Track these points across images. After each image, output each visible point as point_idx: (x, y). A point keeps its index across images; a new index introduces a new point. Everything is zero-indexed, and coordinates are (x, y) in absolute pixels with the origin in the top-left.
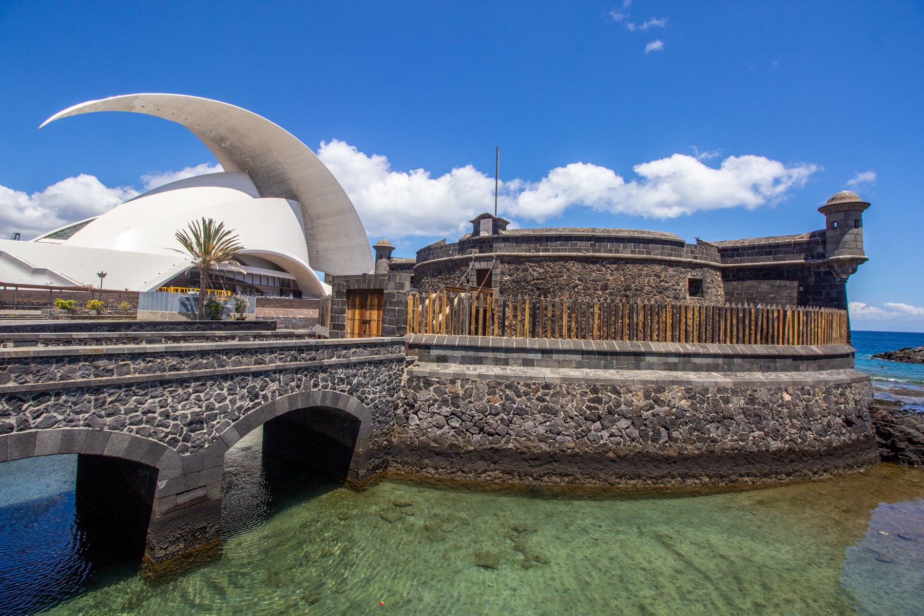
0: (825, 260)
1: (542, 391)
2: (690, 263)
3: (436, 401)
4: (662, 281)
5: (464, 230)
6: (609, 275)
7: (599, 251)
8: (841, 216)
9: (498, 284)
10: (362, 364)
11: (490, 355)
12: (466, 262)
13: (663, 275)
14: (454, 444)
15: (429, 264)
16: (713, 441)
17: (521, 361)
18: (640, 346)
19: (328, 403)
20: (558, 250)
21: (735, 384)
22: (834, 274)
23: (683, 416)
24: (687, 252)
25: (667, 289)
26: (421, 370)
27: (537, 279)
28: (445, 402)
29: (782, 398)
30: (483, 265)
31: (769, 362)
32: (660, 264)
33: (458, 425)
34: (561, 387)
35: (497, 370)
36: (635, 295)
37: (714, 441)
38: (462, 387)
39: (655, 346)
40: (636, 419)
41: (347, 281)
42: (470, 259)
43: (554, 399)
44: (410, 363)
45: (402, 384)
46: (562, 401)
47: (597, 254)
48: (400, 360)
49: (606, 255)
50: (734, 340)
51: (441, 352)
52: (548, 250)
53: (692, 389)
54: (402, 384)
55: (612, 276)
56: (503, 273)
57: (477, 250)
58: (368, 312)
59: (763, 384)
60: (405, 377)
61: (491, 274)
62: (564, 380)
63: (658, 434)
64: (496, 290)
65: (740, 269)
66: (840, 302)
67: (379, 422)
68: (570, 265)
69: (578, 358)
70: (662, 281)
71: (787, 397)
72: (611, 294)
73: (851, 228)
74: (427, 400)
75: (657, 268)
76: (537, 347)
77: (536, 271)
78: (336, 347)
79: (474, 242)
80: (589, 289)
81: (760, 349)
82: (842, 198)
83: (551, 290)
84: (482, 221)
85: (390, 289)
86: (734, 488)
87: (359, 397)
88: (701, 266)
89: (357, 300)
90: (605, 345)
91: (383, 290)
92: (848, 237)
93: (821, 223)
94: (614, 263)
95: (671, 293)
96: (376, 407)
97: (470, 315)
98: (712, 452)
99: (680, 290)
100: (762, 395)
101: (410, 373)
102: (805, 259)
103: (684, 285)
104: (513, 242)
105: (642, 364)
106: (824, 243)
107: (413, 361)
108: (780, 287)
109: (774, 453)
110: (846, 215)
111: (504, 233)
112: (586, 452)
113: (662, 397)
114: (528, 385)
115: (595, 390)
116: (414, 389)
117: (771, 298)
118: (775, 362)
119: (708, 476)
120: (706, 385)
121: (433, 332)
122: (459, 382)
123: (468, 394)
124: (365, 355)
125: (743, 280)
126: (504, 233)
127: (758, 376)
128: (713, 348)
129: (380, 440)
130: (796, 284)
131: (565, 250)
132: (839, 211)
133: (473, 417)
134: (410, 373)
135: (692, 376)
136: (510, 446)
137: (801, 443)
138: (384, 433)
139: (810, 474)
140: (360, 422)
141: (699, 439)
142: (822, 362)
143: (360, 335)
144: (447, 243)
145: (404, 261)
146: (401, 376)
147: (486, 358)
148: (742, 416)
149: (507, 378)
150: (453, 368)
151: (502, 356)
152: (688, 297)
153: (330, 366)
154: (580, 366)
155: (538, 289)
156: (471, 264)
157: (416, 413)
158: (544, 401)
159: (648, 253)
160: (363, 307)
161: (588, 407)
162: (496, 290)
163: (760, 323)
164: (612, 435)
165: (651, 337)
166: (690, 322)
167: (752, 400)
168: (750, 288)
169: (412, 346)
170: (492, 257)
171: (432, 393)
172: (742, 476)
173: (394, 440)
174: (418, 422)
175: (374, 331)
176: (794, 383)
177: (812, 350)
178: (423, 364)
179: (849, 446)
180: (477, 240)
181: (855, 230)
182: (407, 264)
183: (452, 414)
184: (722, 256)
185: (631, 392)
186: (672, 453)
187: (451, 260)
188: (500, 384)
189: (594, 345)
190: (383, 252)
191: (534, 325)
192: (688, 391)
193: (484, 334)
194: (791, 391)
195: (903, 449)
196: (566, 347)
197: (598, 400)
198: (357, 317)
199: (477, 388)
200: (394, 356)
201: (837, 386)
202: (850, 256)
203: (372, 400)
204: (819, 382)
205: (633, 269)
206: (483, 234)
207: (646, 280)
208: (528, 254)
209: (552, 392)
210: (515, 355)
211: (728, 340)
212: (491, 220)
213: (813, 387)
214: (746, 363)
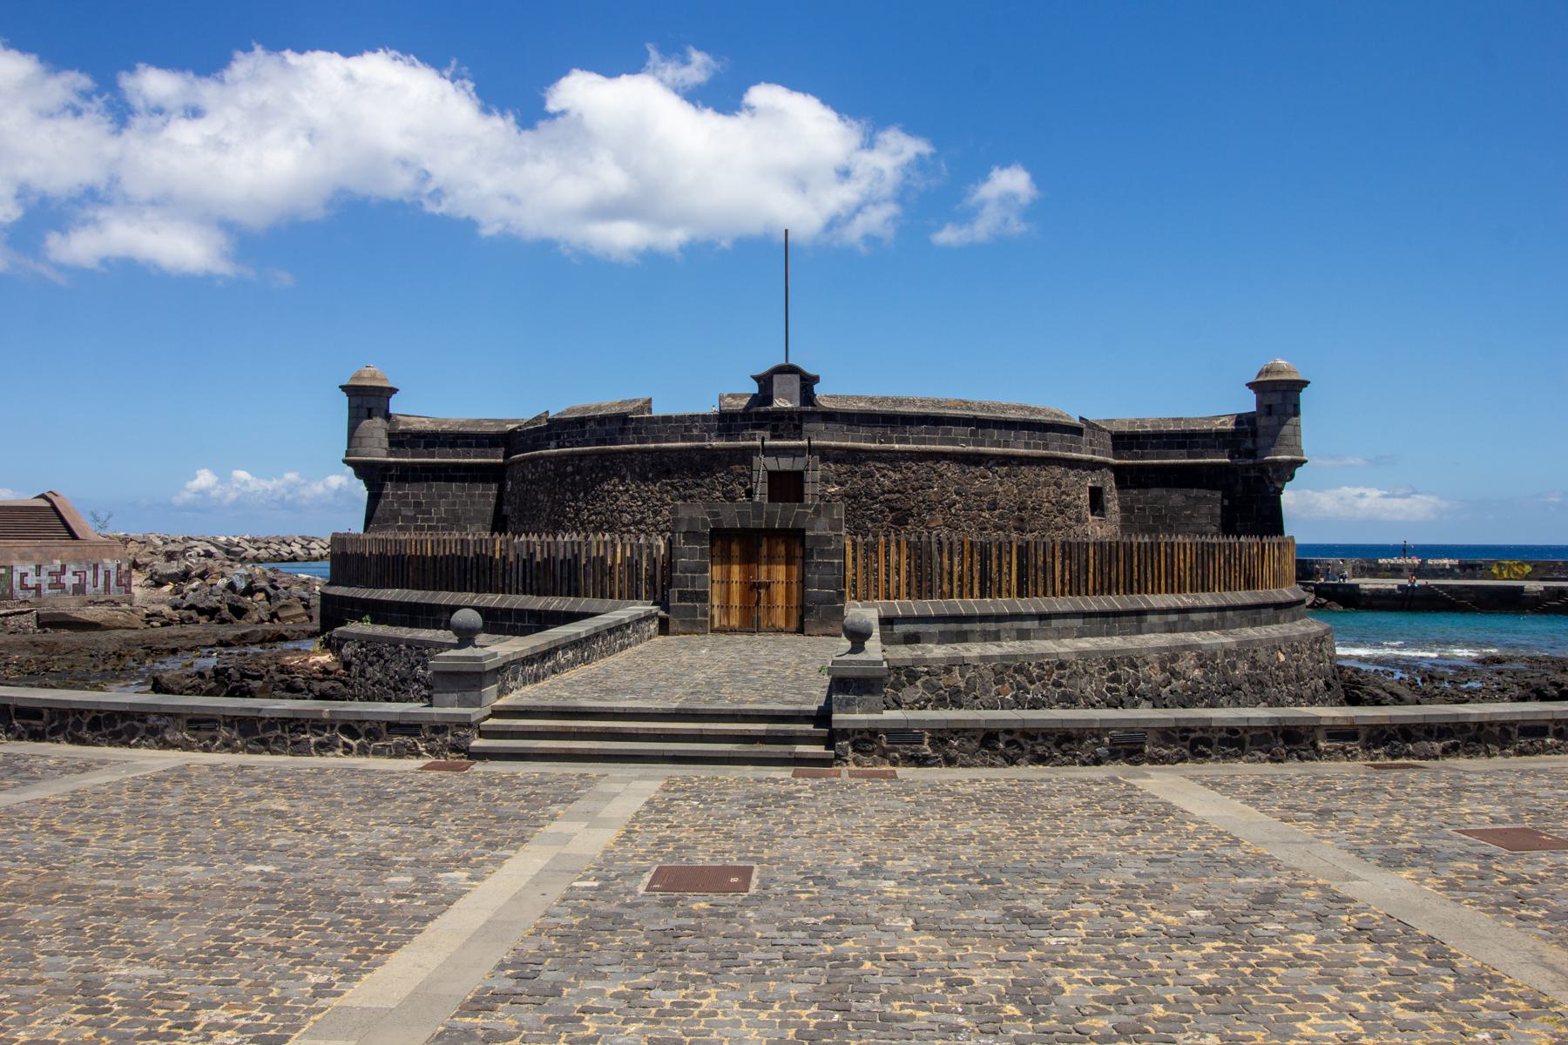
2: (1090, 461)
3: (929, 700)
8: (1275, 399)
11: (977, 627)
15: (630, 452)
21: (1239, 644)
27: (890, 492)
30: (785, 464)
35: (992, 649)
36: (1033, 518)
42: (754, 450)
46: (1082, 683)
47: (982, 449)
49: (994, 450)
52: (906, 441)
55: (1001, 486)
56: (826, 480)
57: (767, 434)
58: (764, 568)
66: (1271, 522)
68: (943, 466)
69: (1078, 622)
75: (1058, 471)
76: (1033, 610)
77: (887, 478)
79: (757, 413)
81: (1244, 597)
82: (1279, 372)
83: (915, 511)
84: (776, 378)
89: (735, 549)
91: (803, 531)
92: (1286, 430)
93: (1248, 403)
94: (1004, 464)
105: (1144, 625)
110: (1279, 397)
114: (1040, 666)
127: (1251, 633)
128: (1206, 599)
130: (1218, 494)
131: (933, 442)
132: (1275, 391)
151: (992, 627)
154: (1081, 634)
155: (892, 510)
158: (1060, 685)
159: (1046, 447)
160: (750, 559)
161: (1109, 689)
176: (1286, 639)
180: (768, 413)
184: (1116, 447)
187: (702, 449)
188: (1007, 667)
192: (1199, 657)
206: (779, 403)
208: (873, 446)
209: (1067, 672)
210: (1007, 625)
212: (795, 381)
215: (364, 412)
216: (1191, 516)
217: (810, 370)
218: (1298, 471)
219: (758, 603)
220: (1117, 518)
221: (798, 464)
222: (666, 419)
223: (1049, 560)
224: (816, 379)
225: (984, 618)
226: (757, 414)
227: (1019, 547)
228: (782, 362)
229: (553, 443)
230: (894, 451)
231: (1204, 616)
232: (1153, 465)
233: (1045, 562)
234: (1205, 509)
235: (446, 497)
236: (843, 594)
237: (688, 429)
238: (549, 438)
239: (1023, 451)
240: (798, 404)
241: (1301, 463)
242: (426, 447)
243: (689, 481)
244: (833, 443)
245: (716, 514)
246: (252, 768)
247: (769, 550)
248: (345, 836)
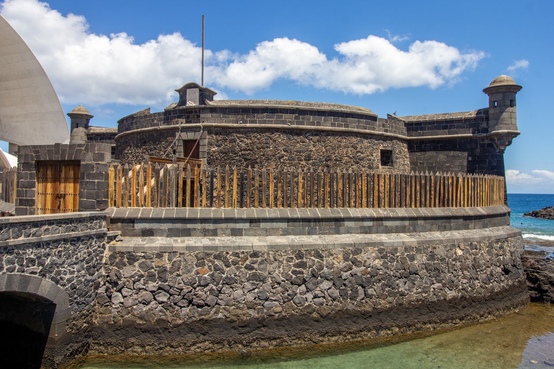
0: (488, 134)
1: (250, 259)
2: (381, 135)
3: (142, 276)
4: (358, 152)
5: (171, 99)
6: (311, 146)
7: (302, 123)
8: (500, 97)
9: (206, 155)
10: (57, 242)
11: (199, 226)
12: (172, 132)
13: (359, 146)
14: (163, 320)
15: (133, 133)
16: (401, 295)
17: (229, 231)
18: (340, 212)
19: (15, 288)
20: (265, 122)
21: (419, 243)
22: (495, 146)
23: (377, 274)
24: (379, 126)
25: (362, 159)
26: (124, 244)
27: (244, 150)
28: (151, 277)
29: (455, 253)
30: (190, 136)
31: (445, 222)
32: (357, 136)
33: (165, 299)
34: (268, 254)
35: (205, 241)
36: (335, 165)
37: (403, 294)
38: (170, 260)
39: (354, 212)
40: (336, 280)
41: (37, 152)
42: (177, 129)
43: (262, 266)
44: (111, 238)
45: (104, 261)
46: (270, 268)
48: (101, 236)
50: (418, 204)
51: (147, 226)
52: (255, 122)
53: (384, 249)
54: (104, 261)
55: (315, 147)
56: (210, 144)
57: (184, 120)
58: (62, 185)
59: (441, 242)
60: (107, 253)
61: (198, 145)
62: (271, 247)
63: (357, 292)
64: (203, 161)
65: (422, 141)
66: (499, 170)
67: (78, 303)
68: (276, 136)
69: (284, 225)
70: (358, 152)
71: (460, 252)
72: (314, 164)
73: (507, 107)
74: (132, 277)
75: (354, 140)
76: (245, 216)
77: (243, 142)
78: (24, 224)
79: (180, 112)
80: (294, 160)
81: (438, 211)
82: (501, 81)
83: (258, 160)
84: (188, 90)
85: (88, 160)
86: (420, 335)
87: (53, 279)
88: (391, 138)
89: (49, 173)
90: (309, 213)
91: (80, 161)
92: (505, 115)
93: (484, 102)
94: (316, 135)
95: (365, 163)
96: (73, 287)
97: (178, 186)
98: (401, 304)
100: (441, 251)
101: (112, 249)
102: (473, 133)
103: (377, 156)
104: (220, 112)
105: (342, 229)
106: (487, 119)
107: (115, 237)
108: (454, 157)
109: (450, 301)
110: (504, 96)
111: (211, 103)
112: (292, 315)
113: (359, 258)
114: (236, 255)
115: (300, 256)
116: (117, 265)
117: (447, 167)
118: (450, 223)
119: (398, 326)
120: (395, 245)
121: (138, 205)
122: (166, 256)
123: (176, 267)
124: (60, 232)
125: (425, 151)
126: (211, 103)
127: (437, 235)
128: (401, 212)
129: (79, 323)
130: (466, 154)
131: (271, 122)
132: (498, 93)
133: (181, 290)
134: (112, 249)
135: (384, 238)
136: (220, 315)
137: (471, 291)
138: (83, 315)
139: (478, 317)
140: (55, 305)
141: (390, 294)
142: (486, 220)
143: (53, 211)
144: (152, 112)
145: (103, 130)
146: (103, 252)
147: (194, 229)
148: (425, 271)
149: (216, 248)
150: (160, 241)
151: (211, 226)
152: (380, 167)
153: (17, 246)
154: (286, 233)
155: (246, 160)
156: (178, 134)
157: (120, 291)
158: (252, 268)
159: (346, 126)
160: (56, 179)
161: (294, 272)
162: (203, 161)
163: (438, 188)
164: (315, 297)
165: (349, 204)
166: (382, 189)
167: (432, 257)
168: (430, 158)
169: (114, 221)
170: (200, 127)
171: (137, 268)
172: (425, 323)
173: (95, 321)
174: (122, 300)
175: (70, 206)
176: (465, 240)
177: (478, 211)
178: (127, 238)
179: (506, 291)
180: (184, 109)
181: (510, 109)
182: (107, 134)
183: (160, 288)
184: (408, 130)
185: (332, 255)
186: (368, 308)
188: (208, 255)
189: (298, 213)
190: (79, 120)
191: (242, 195)
192: (381, 251)
193: (192, 205)
194: (462, 247)
195: (547, 291)
196: (273, 215)
197: (303, 265)
198: (49, 190)
199: (185, 260)
200: (93, 232)
201: (497, 241)
202: (506, 131)
203: (69, 281)
204: (484, 238)
205: (332, 140)
206: (190, 104)
207: (345, 151)
208: (235, 125)
209: (259, 259)
210: (224, 225)
211: (413, 204)
212: (197, 90)
213: (479, 242)
214: (428, 224)
215: (75, 125)
216: (450, 166)
219: (59, 207)
221: (196, 136)
225: (204, 220)
226: (179, 110)
230: (246, 128)
231: (398, 223)
232: (428, 139)
234: (457, 163)
237: (153, 121)
239: (329, 128)
240: (198, 104)
241: (517, 134)
242: (100, 140)
243: (152, 147)
244: (214, 124)
247: (66, 173)
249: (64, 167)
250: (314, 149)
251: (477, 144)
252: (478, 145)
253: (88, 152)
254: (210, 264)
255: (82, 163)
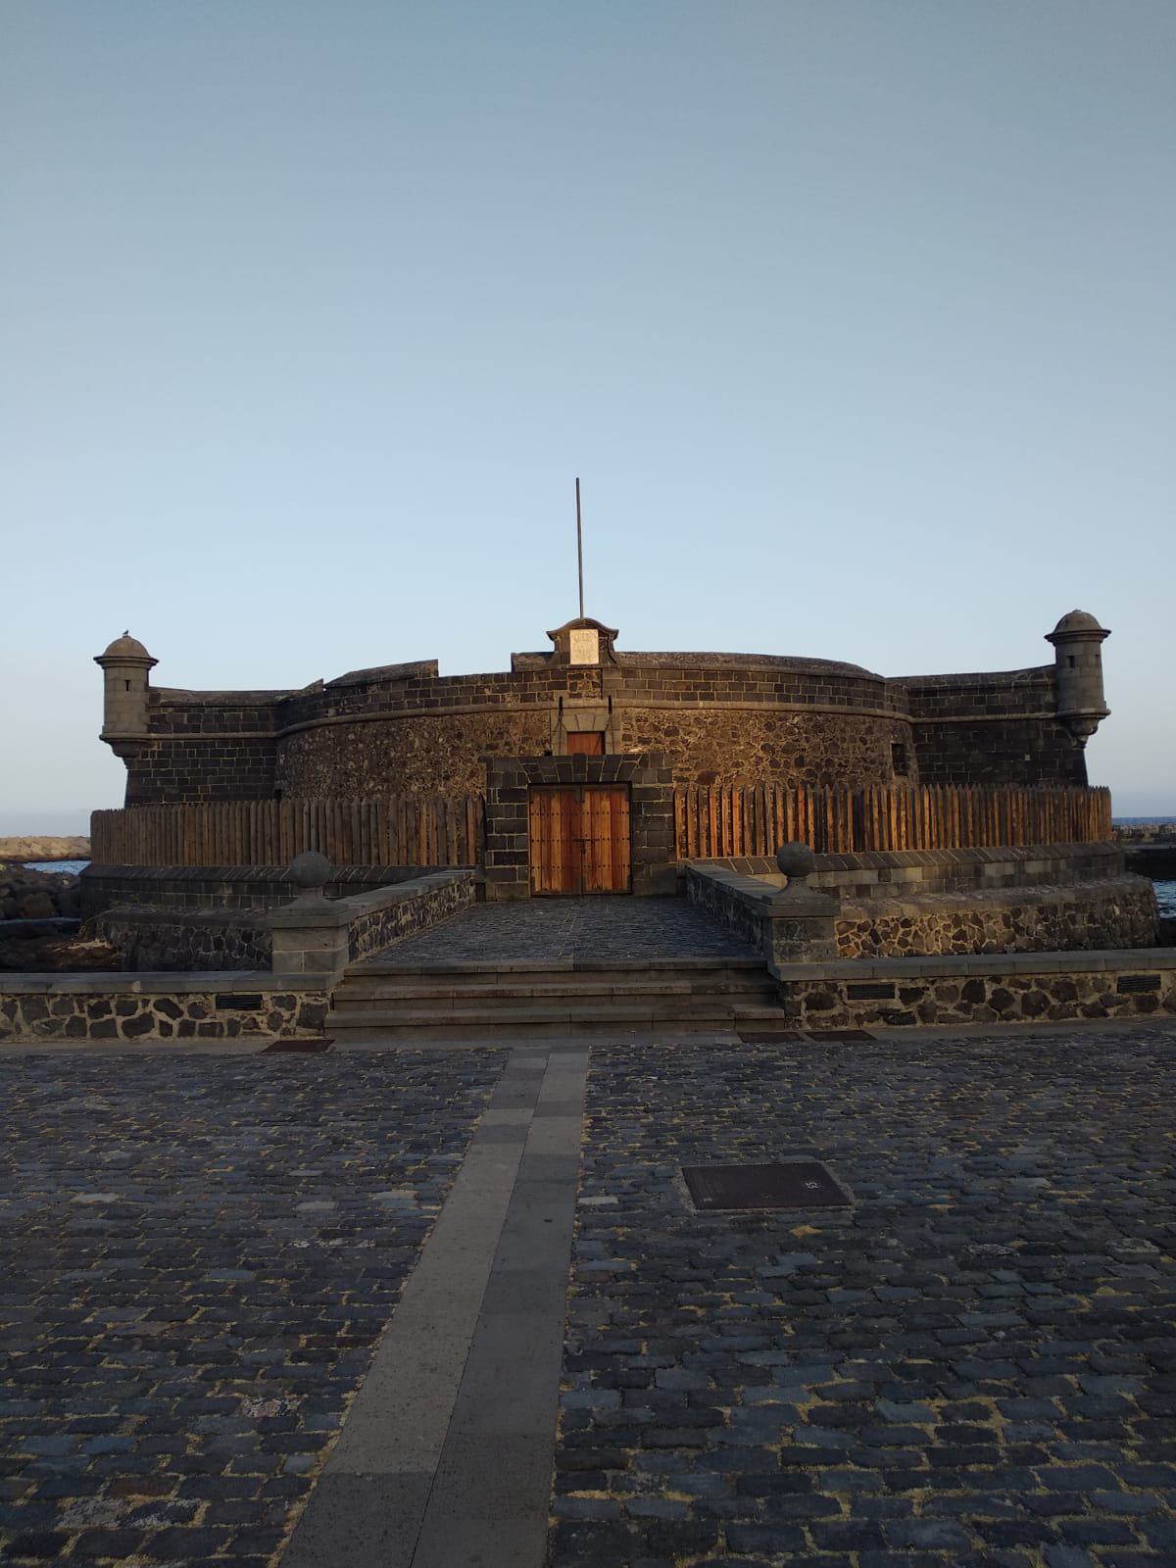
1: (901, 930)
17: (854, 890)
25: (873, 762)
34: (922, 921)
83: (721, 769)
84: (573, 633)
91: (630, 783)
99: (886, 764)
159: (850, 703)
192: (1041, 911)
206: (575, 661)
209: (913, 928)
212: (595, 633)
217: (609, 625)
218: (1101, 724)
220: (916, 776)
222: (456, 679)
223: (885, 810)
224: (615, 634)
227: (854, 798)
228: (577, 616)
229: (332, 711)
233: (880, 813)
235: (213, 772)
236: (674, 849)
237: (480, 690)
238: (327, 706)
239: (827, 707)
245: (535, 768)
246: (45, 1058)
248: (205, 1143)
249: (587, 796)
250: (806, 746)
251: (1038, 730)
252: (1041, 733)
253: (646, 766)
254: (857, 940)
255: (636, 786)
